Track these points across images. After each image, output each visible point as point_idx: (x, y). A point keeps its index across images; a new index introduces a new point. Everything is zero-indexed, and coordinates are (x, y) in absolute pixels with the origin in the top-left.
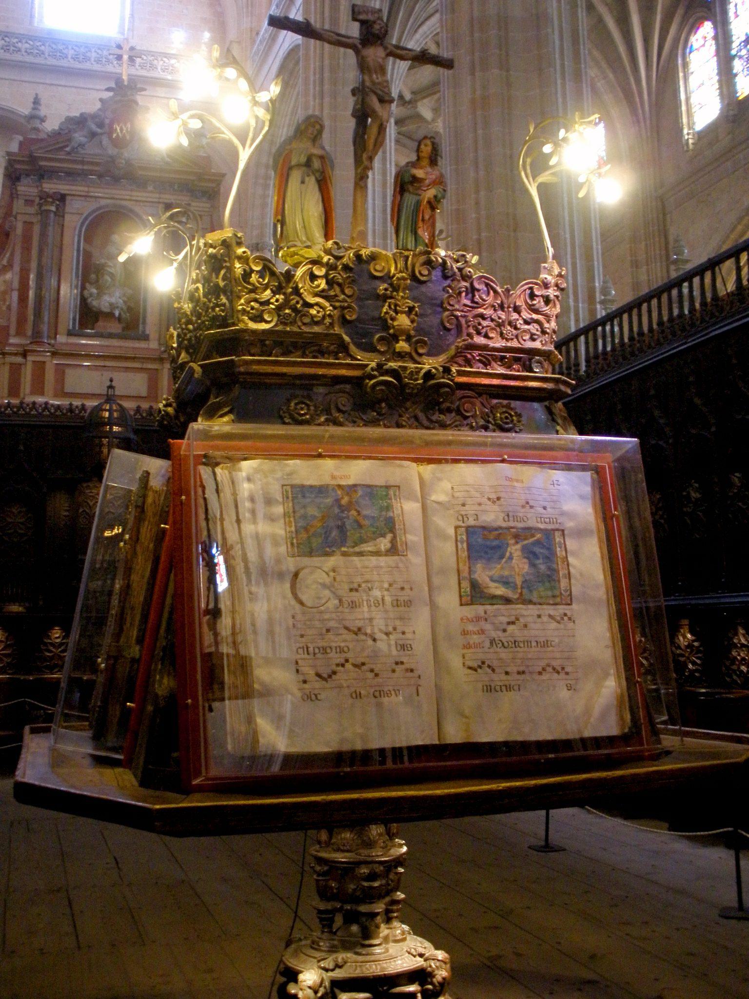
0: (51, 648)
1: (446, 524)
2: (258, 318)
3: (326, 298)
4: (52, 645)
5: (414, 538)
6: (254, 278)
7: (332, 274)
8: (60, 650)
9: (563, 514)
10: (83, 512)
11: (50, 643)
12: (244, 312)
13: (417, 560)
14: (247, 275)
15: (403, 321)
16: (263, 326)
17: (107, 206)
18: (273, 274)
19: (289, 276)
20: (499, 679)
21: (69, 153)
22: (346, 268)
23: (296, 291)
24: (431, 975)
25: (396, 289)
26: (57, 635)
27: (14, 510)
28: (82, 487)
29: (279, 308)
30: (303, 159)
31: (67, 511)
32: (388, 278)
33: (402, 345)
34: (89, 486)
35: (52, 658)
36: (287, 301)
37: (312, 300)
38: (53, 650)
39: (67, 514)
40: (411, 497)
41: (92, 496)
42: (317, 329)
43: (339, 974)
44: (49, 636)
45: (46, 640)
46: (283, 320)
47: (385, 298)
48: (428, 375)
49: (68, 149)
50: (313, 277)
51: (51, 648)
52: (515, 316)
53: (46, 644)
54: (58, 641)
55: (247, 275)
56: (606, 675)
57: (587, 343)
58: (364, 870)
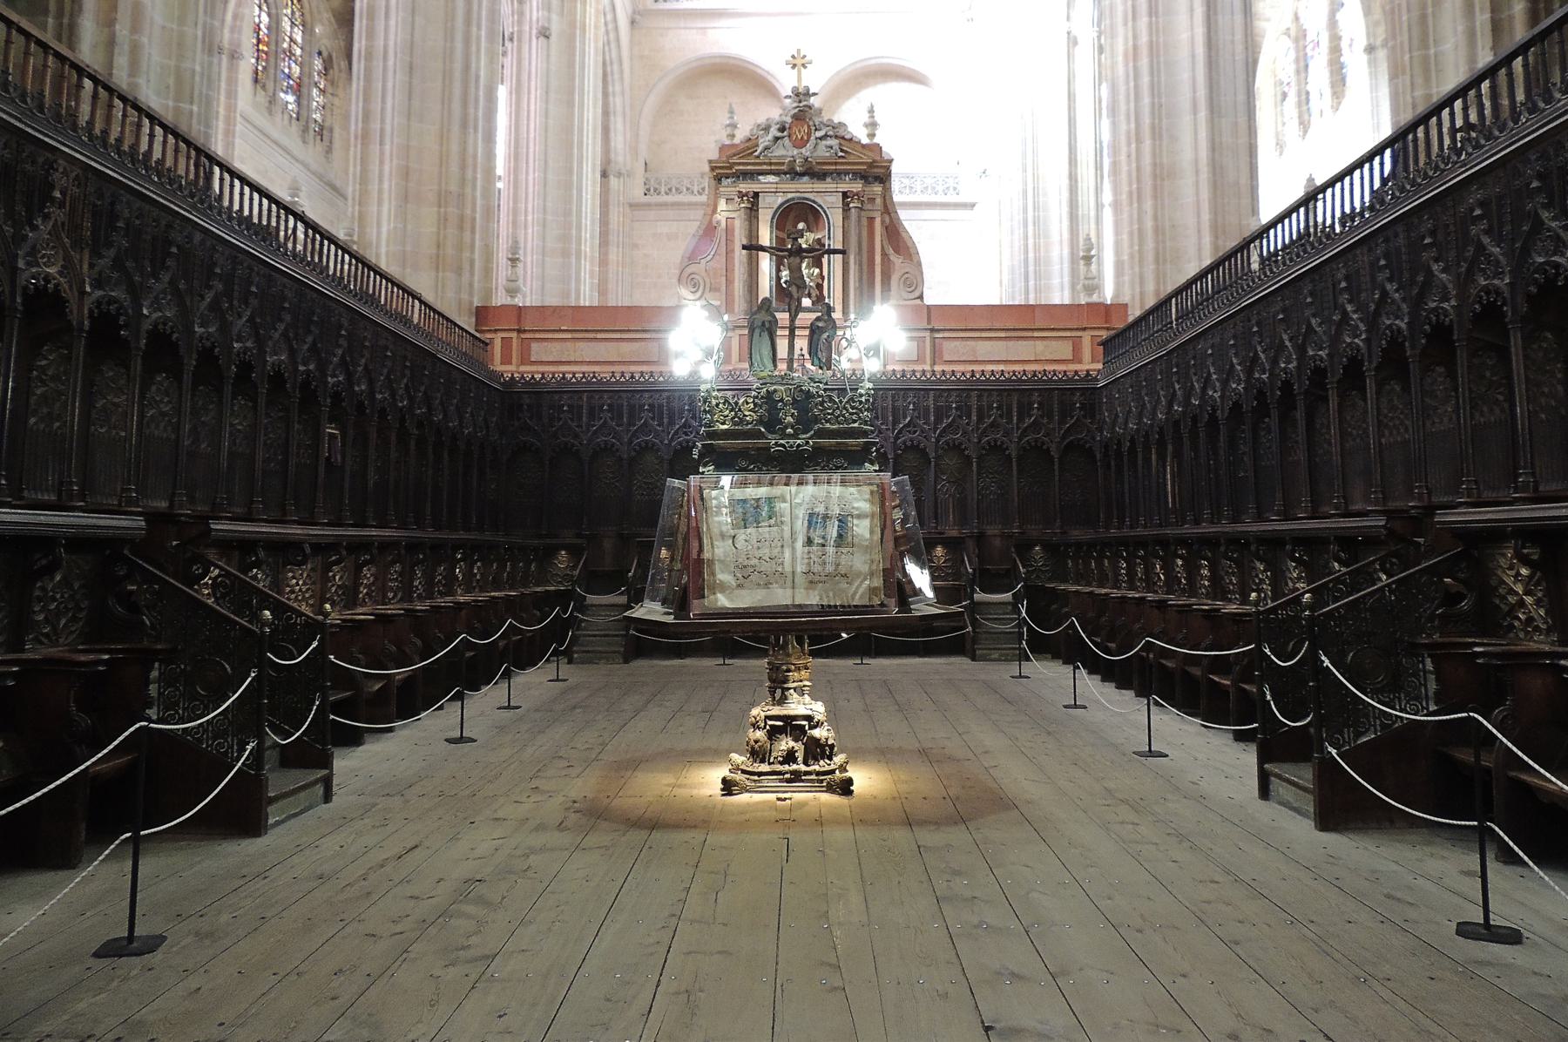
1: (801, 513)
2: (723, 424)
3: (755, 412)
5: (787, 519)
6: (721, 406)
7: (756, 401)
9: (853, 508)
12: (717, 421)
13: (787, 529)
14: (717, 405)
15: (789, 419)
16: (725, 427)
17: (793, 199)
18: (729, 403)
19: (736, 403)
20: (817, 578)
21: (758, 157)
22: (762, 397)
23: (740, 410)
24: (813, 718)
25: (785, 405)
29: (732, 419)
30: (760, 324)
32: (782, 400)
33: (789, 430)
36: (736, 414)
37: (747, 413)
40: (785, 501)
42: (750, 426)
43: (769, 713)
46: (735, 424)
47: (781, 409)
48: (799, 445)
49: (756, 154)
50: (747, 403)
52: (844, 412)
55: (717, 405)
56: (865, 579)
57: (1177, 304)
58: (784, 668)
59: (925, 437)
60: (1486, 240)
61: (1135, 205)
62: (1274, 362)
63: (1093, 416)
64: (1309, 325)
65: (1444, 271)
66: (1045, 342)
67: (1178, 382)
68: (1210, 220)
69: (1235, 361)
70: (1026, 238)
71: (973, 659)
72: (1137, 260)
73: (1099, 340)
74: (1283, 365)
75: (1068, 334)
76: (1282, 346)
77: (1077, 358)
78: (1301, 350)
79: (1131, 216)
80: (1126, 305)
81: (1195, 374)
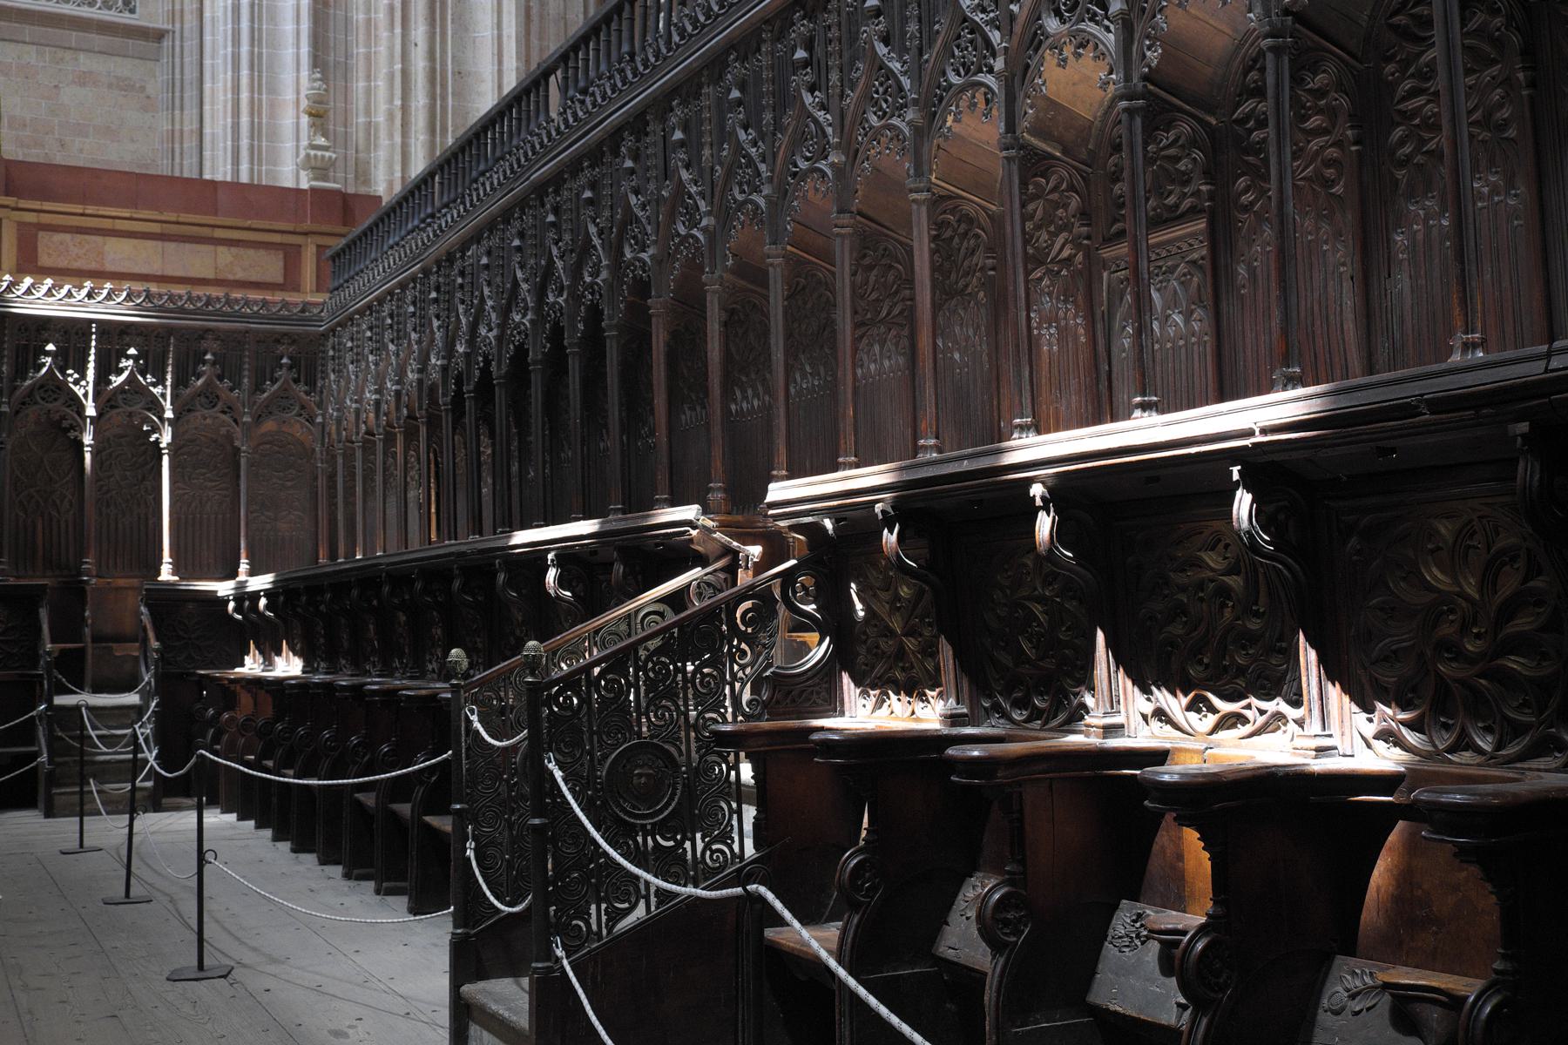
60: (881, 49)
61: (398, 30)
62: (576, 273)
63: (311, 383)
64: (628, 208)
65: (823, 107)
66: (234, 250)
67: (438, 317)
68: (517, 69)
69: (519, 275)
70: (236, 89)
71: (49, 814)
72: (398, 122)
73: (329, 253)
74: (588, 279)
75: (277, 238)
76: (588, 246)
77: (291, 282)
78: (616, 252)
79: (391, 49)
80: (380, 197)
81: (463, 302)
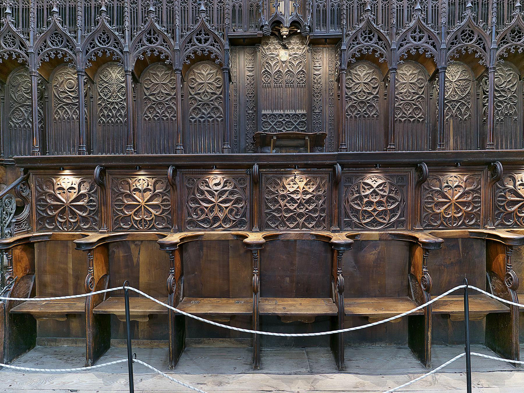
0: (209, 197)
4: (211, 193)
8: (221, 199)
10: (264, 72)
11: (206, 191)
26: (217, 181)
27: (204, 72)
28: (264, 49)
31: (250, 71)
34: (270, 48)
35: (211, 210)
38: (213, 200)
39: (249, 74)
41: (273, 57)
44: (206, 182)
45: (202, 188)
51: (209, 197)
53: (202, 193)
54: (219, 188)
59: (433, 45)
